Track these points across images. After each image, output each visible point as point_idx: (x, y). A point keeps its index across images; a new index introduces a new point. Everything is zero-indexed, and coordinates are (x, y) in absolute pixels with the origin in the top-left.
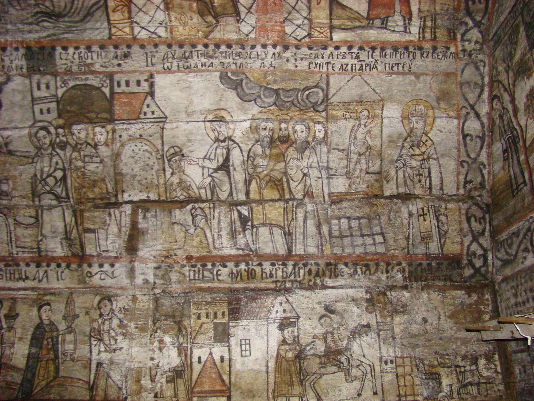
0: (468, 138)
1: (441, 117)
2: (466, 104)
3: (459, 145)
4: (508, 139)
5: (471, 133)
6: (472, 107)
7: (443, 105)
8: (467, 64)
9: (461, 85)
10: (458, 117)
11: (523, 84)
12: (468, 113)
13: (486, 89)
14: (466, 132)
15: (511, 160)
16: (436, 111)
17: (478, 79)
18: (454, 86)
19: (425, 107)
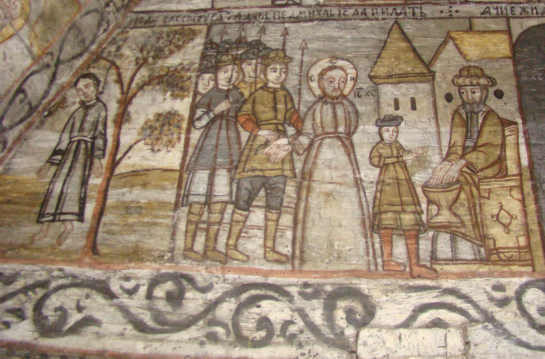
0: (21, 96)
1: (23, 41)
2: (56, 53)
3: (6, 95)
4: (79, 142)
5: (29, 92)
6: (58, 63)
7: (39, 29)
8: (96, 10)
9: (74, 26)
10: (36, 60)
11: (160, 97)
12: (48, 66)
13: (86, 56)
14: (25, 87)
15: (65, 170)
16: (27, 28)
17: (89, 37)
18: (66, 19)
19: (23, 8)
